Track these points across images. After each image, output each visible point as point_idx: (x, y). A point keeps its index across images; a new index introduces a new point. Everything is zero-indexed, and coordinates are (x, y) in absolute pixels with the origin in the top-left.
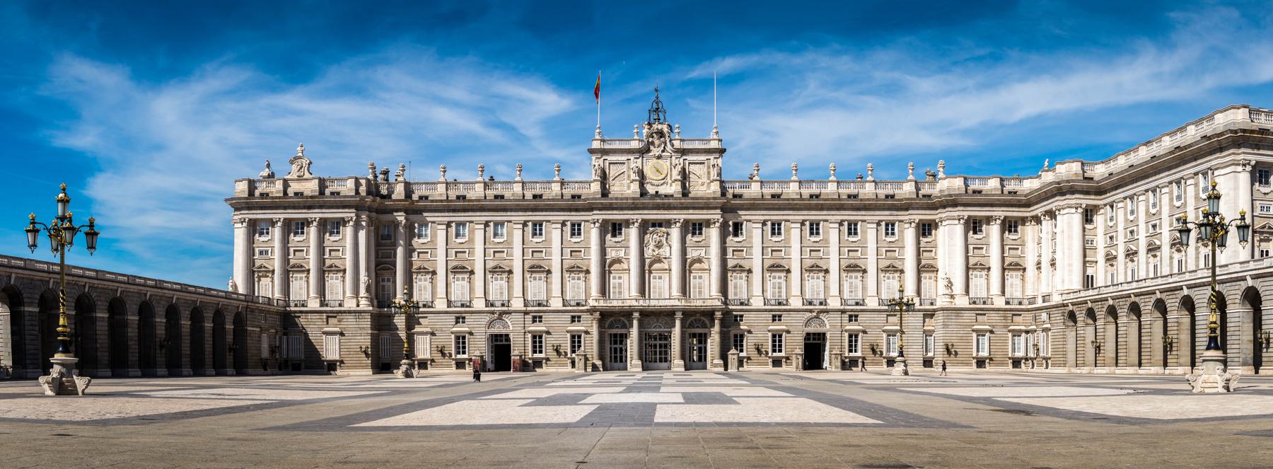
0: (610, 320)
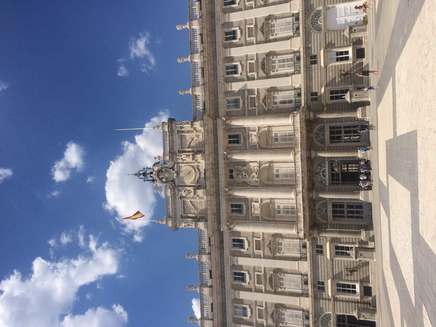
0: (319, 218)
